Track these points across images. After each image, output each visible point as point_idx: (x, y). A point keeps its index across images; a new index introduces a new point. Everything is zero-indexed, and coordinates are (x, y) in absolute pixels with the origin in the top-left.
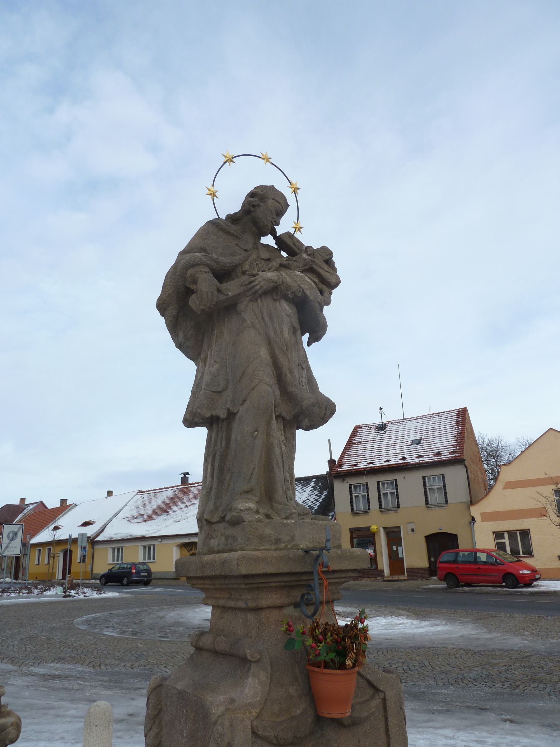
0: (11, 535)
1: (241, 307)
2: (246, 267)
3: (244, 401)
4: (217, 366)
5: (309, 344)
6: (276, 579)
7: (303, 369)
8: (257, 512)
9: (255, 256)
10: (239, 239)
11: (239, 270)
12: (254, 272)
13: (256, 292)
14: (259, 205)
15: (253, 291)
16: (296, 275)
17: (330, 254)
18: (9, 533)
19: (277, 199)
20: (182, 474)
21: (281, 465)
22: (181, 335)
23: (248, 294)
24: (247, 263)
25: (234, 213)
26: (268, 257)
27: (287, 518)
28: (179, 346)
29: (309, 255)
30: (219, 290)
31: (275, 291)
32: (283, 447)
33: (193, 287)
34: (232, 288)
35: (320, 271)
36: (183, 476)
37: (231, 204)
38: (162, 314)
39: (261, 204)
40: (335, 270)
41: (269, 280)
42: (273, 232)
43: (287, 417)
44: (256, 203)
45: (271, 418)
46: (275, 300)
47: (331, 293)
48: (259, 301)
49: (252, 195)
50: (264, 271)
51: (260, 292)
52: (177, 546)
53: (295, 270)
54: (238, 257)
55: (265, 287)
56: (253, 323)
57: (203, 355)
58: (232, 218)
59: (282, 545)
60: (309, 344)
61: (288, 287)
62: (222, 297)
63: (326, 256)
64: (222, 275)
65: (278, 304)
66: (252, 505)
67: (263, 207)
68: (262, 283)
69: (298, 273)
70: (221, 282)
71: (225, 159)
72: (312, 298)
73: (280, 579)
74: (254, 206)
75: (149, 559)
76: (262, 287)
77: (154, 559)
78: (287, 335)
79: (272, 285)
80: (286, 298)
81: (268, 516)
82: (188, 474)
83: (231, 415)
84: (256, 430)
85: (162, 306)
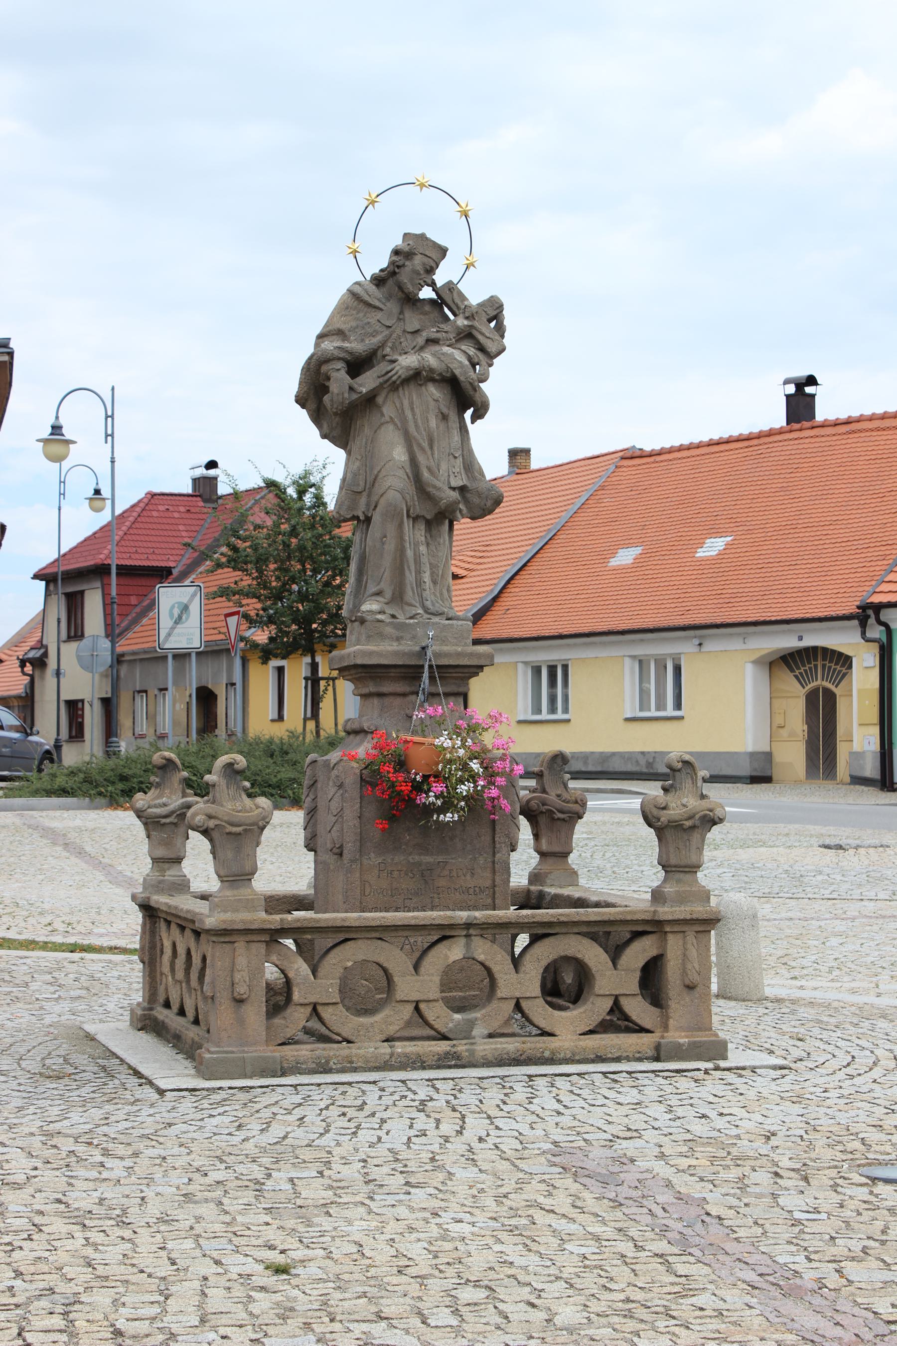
0: (176, 612)
1: (380, 400)
2: (388, 350)
3: (376, 506)
4: (357, 464)
5: (472, 423)
6: (393, 670)
7: (455, 457)
8: (382, 612)
9: (399, 331)
10: (381, 310)
11: (379, 353)
12: (395, 357)
13: (394, 382)
14: (404, 265)
15: (390, 382)
16: (443, 354)
17: (500, 307)
18: (173, 607)
19: (427, 253)
20: (787, 382)
21: (413, 568)
22: (325, 426)
23: (385, 386)
24: (390, 344)
25: (382, 270)
26: (418, 327)
27: (411, 618)
28: (324, 436)
29: (467, 318)
30: (351, 389)
31: (417, 377)
32: (423, 549)
33: (327, 384)
34: (367, 382)
35: (480, 337)
36: (791, 389)
37: (377, 261)
38: (303, 407)
39: (407, 263)
40: (500, 330)
41: (408, 368)
42: (433, 284)
43: (429, 517)
44: (401, 263)
45: (402, 523)
46: (421, 385)
47: (491, 365)
48: (401, 389)
49: (396, 252)
50: (406, 353)
51: (398, 382)
52: (757, 662)
53: (444, 344)
54: (379, 338)
55: (403, 377)
56: (391, 418)
57: (349, 448)
58: (379, 280)
59: (403, 642)
60: (472, 423)
61: (432, 370)
62: (355, 396)
63: (494, 311)
64: (357, 366)
65: (423, 388)
66: (375, 607)
67: (415, 258)
68: (400, 373)
69: (446, 349)
70: (353, 377)
71: (366, 203)
72: (462, 378)
73: (398, 670)
74: (398, 267)
75: (661, 706)
76: (400, 377)
77: (678, 705)
78: (433, 423)
79: (411, 372)
80: (433, 380)
81: (393, 616)
82: (811, 380)
83: (368, 520)
84: (385, 537)
85: (301, 401)
